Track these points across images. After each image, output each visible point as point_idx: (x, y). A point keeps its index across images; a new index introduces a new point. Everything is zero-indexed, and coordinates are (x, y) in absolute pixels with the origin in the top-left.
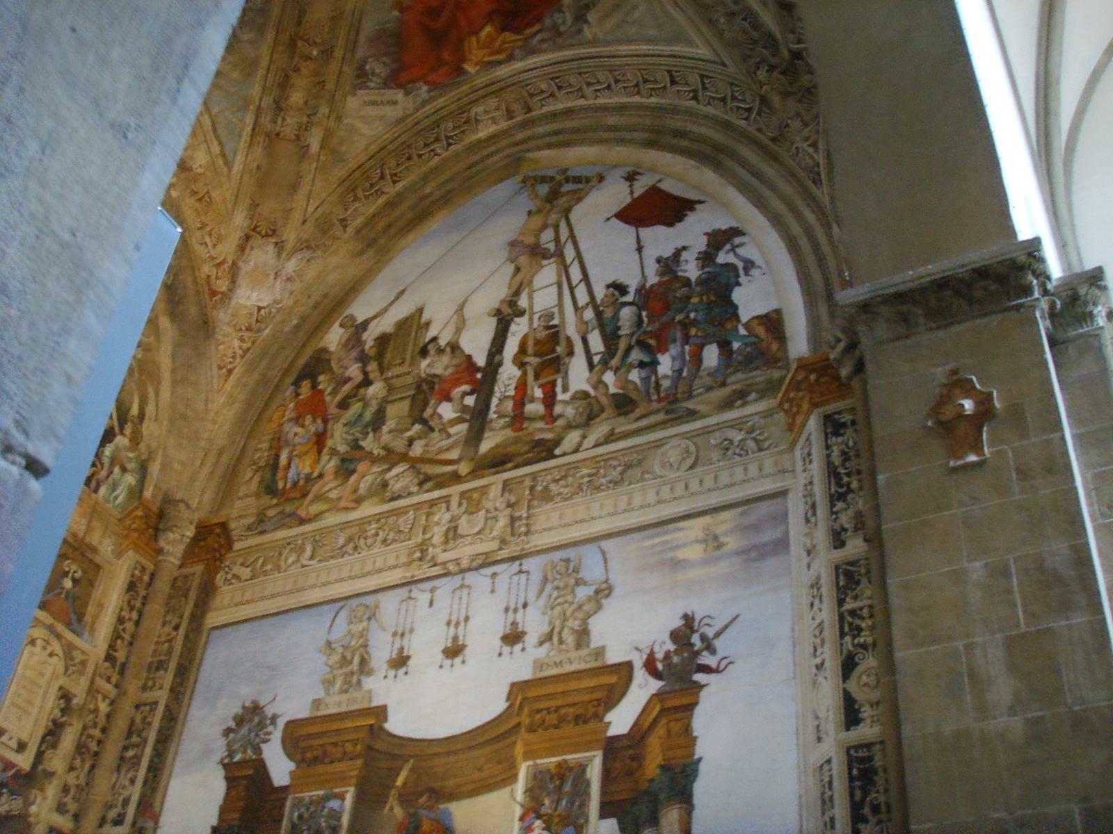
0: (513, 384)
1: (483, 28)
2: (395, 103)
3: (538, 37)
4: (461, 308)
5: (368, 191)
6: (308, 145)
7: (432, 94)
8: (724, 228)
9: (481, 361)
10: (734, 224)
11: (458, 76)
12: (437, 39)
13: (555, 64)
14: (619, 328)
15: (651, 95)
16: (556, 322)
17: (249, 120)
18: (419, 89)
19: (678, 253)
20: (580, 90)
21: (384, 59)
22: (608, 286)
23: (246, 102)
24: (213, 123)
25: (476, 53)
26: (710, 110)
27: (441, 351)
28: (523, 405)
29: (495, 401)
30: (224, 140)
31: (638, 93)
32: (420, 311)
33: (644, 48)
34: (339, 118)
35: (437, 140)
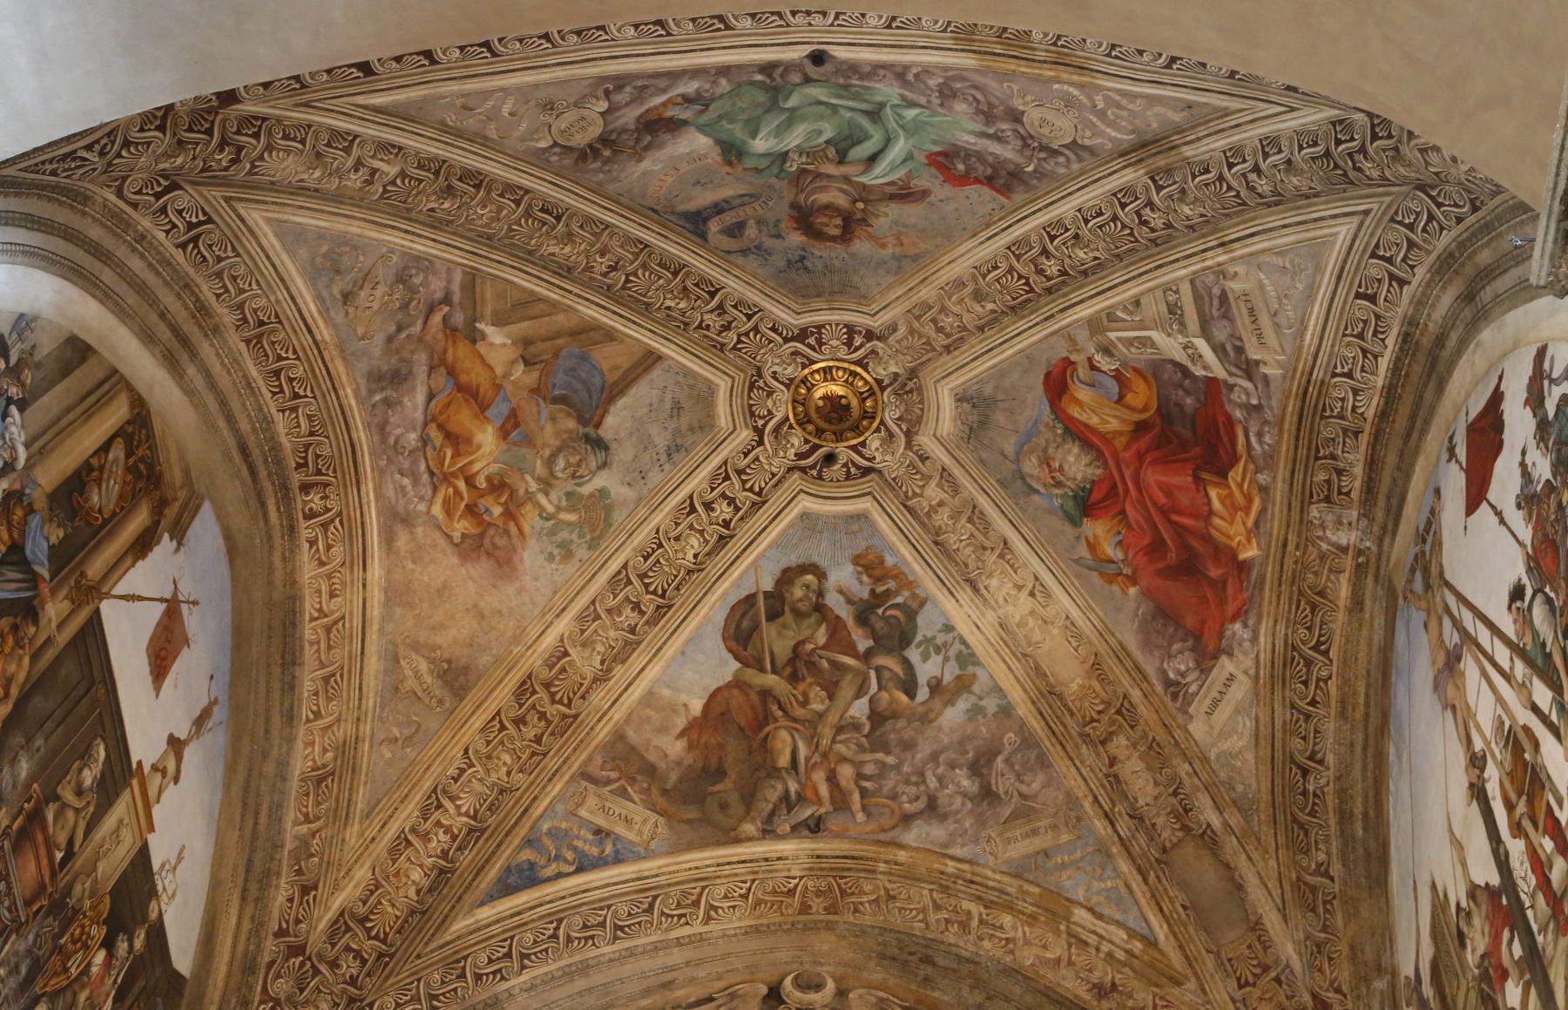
0: (1527, 865)
1: (1209, 503)
2: (1231, 678)
3: (1253, 439)
4: (1451, 832)
5: (1306, 807)
6: (1209, 825)
7: (1251, 623)
8: (1530, 372)
9: (1495, 880)
10: (1534, 352)
11: (1249, 576)
12: (1188, 568)
13: (1297, 439)
14: (1544, 645)
15: (1383, 340)
16: (1507, 724)
17: (1124, 866)
18: (1234, 634)
19: (1523, 465)
20: (1345, 431)
21: (1176, 647)
22: (1510, 608)
23: (1103, 851)
24: (1091, 910)
25: (1232, 530)
26: (1420, 272)
27: (1469, 914)
28: (1549, 881)
29: (1530, 913)
30: (1118, 916)
31: (1376, 357)
32: (1434, 887)
33: (1317, 310)
34: (1205, 760)
35: (1309, 663)
